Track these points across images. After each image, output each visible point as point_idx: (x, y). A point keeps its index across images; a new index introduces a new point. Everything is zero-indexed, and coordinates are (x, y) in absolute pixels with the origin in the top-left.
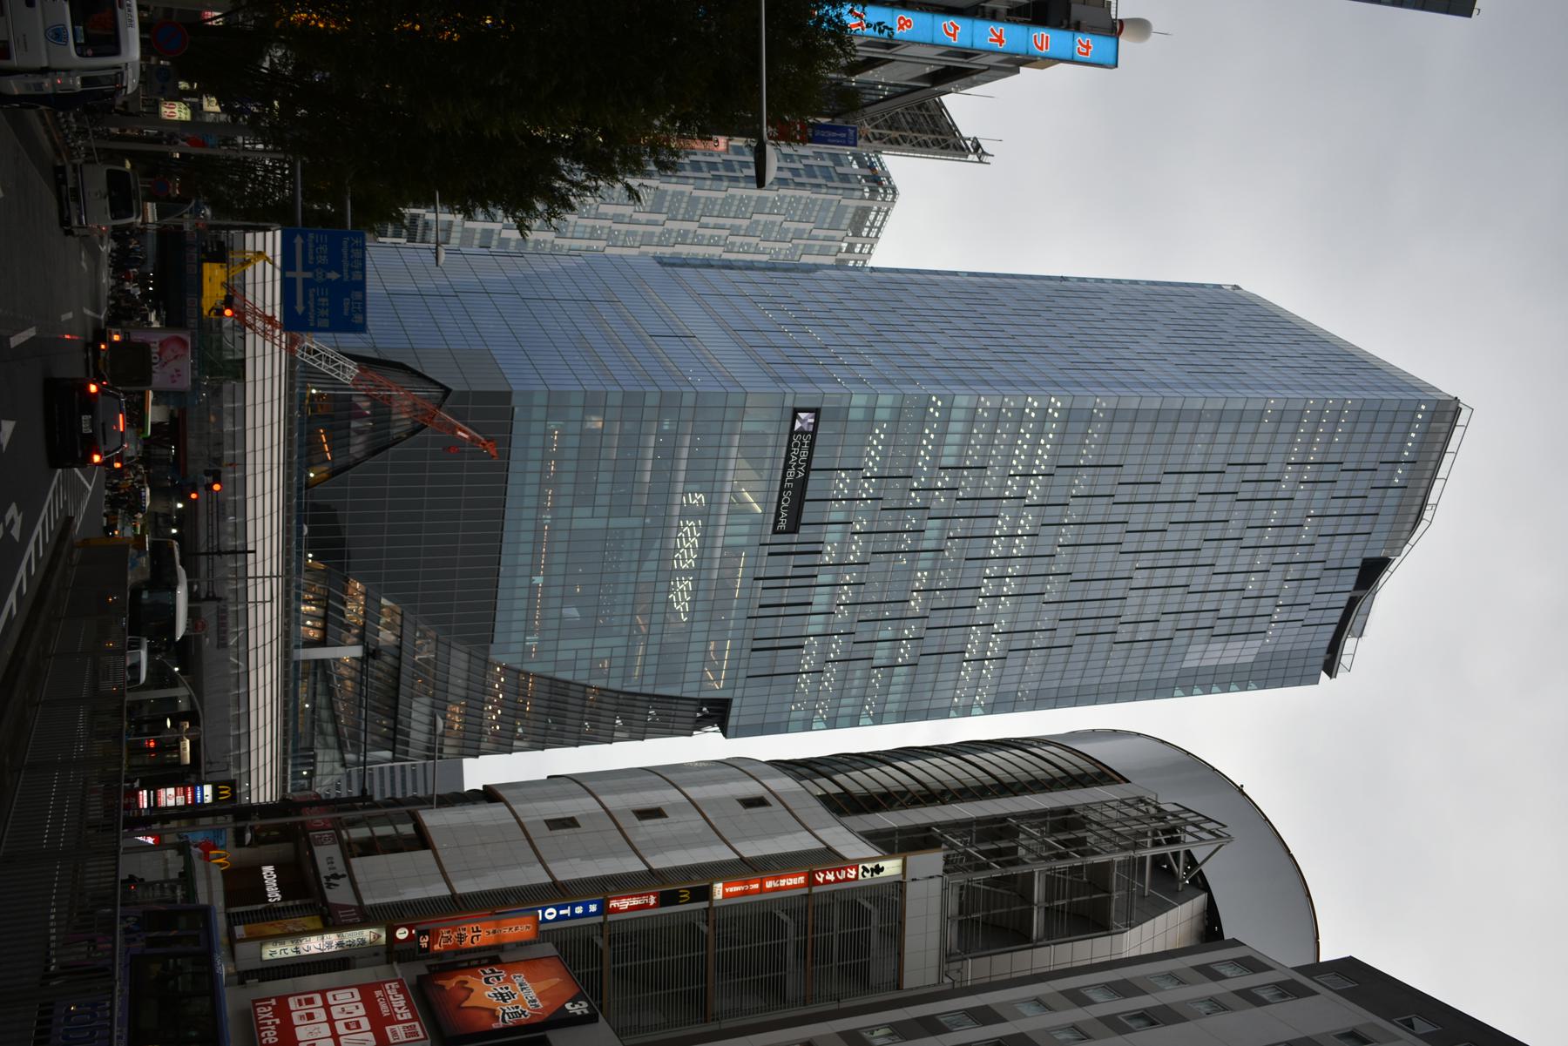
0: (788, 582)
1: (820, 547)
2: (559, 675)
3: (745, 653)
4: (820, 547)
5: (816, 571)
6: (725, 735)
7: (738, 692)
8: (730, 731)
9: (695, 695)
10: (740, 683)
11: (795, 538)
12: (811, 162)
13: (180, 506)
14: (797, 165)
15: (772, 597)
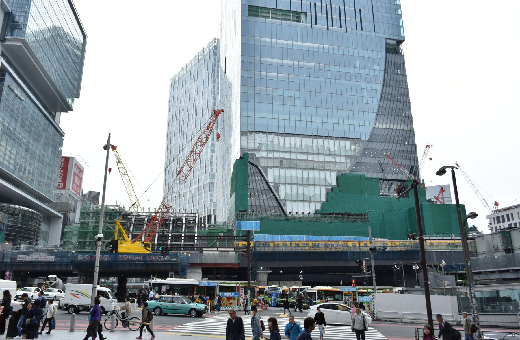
0: (329, 16)
1: (313, 4)
2: (376, 110)
3: (363, 33)
4: (313, 4)
5: (324, 5)
6: (403, 41)
7: (382, 35)
8: (401, 39)
9: (384, 54)
10: (378, 35)
11: (308, 14)
12: (206, 69)
13: (261, 268)
14: (207, 73)
15: (336, 23)
